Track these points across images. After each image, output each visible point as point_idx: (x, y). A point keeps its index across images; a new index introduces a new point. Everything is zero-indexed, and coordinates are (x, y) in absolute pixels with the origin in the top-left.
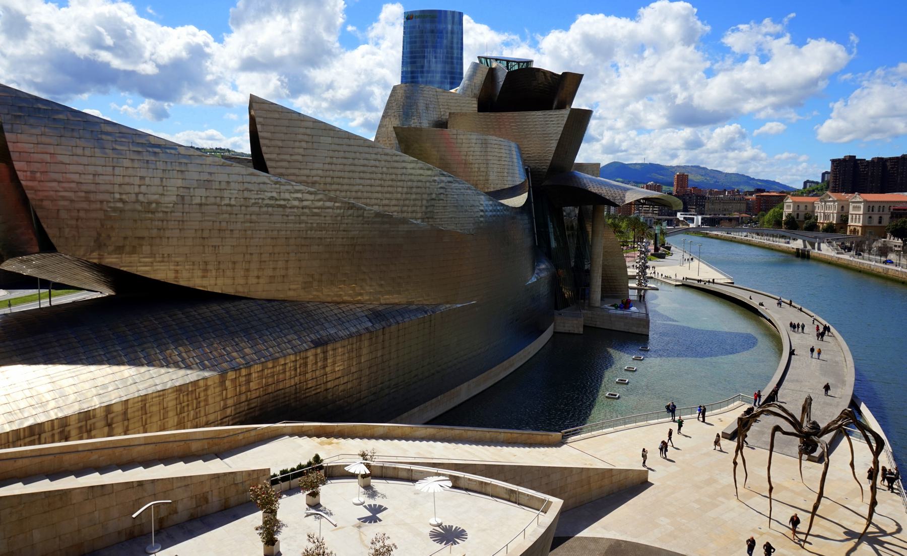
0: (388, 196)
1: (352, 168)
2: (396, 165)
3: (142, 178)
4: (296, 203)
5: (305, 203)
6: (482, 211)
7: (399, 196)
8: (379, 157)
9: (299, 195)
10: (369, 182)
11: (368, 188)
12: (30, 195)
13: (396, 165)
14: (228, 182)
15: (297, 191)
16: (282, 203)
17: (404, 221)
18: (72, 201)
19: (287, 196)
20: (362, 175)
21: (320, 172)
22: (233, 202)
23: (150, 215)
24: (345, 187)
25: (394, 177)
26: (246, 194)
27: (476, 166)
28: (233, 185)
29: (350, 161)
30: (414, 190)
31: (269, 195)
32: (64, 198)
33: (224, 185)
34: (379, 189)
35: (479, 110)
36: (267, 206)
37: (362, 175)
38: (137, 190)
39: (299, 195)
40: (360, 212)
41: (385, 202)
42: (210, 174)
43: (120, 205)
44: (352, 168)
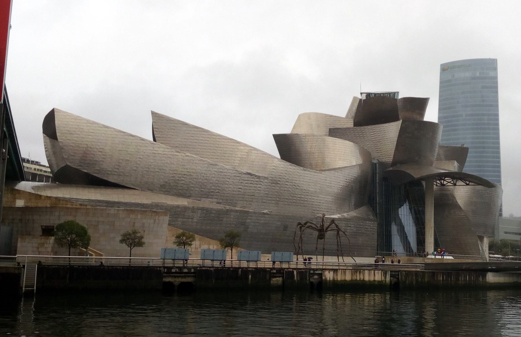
0: (213, 154)
1: (195, 141)
2: (219, 140)
5: (165, 153)
6: (274, 166)
7: (219, 154)
8: (209, 136)
9: (163, 149)
10: (203, 147)
11: (203, 150)
13: (219, 140)
15: (162, 148)
16: (154, 152)
17: (216, 165)
18: (73, 147)
19: (157, 149)
20: (200, 144)
21: (180, 143)
22: (133, 150)
24: (192, 149)
25: (216, 145)
26: (139, 147)
27: (317, 154)
29: (195, 138)
30: (227, 152)
32: (70, 146)
34: (209, 150)
35: (354, 126)
37: (200, 144)
39: (163, 149)
40: (191, 158)
41: (211, 157)
44: (195, 141)
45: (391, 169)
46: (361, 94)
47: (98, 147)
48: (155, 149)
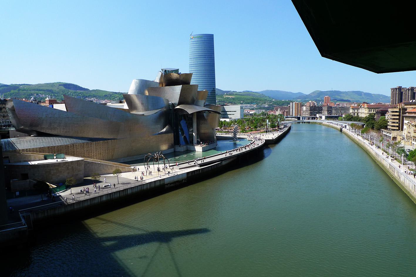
3: (39, 113)
4: (71, 117)
5: (73, 116)
7: (100, 114)
12: (18, 117)
14: (56, 113)
22: (57, 117)
23: (40, 120)
26: (60, 115)
28: (57, 113)
31: (65, 115)
33: (55, 114)
36: (65, 117)
38: (37, 115)
39: (72, 115)
42: (52, 111)
43: (34, 118)
45: (178, 107)
46: (162, 70)
47: (38, 117)
48: (68, 115)
